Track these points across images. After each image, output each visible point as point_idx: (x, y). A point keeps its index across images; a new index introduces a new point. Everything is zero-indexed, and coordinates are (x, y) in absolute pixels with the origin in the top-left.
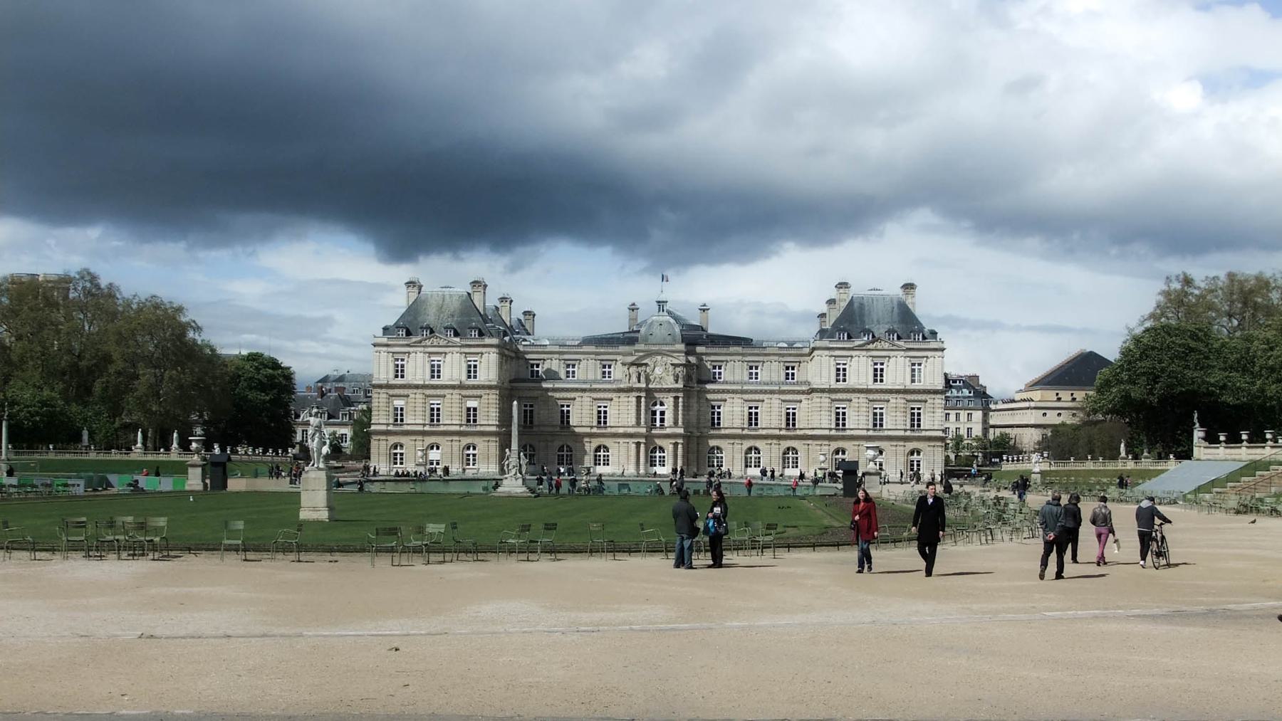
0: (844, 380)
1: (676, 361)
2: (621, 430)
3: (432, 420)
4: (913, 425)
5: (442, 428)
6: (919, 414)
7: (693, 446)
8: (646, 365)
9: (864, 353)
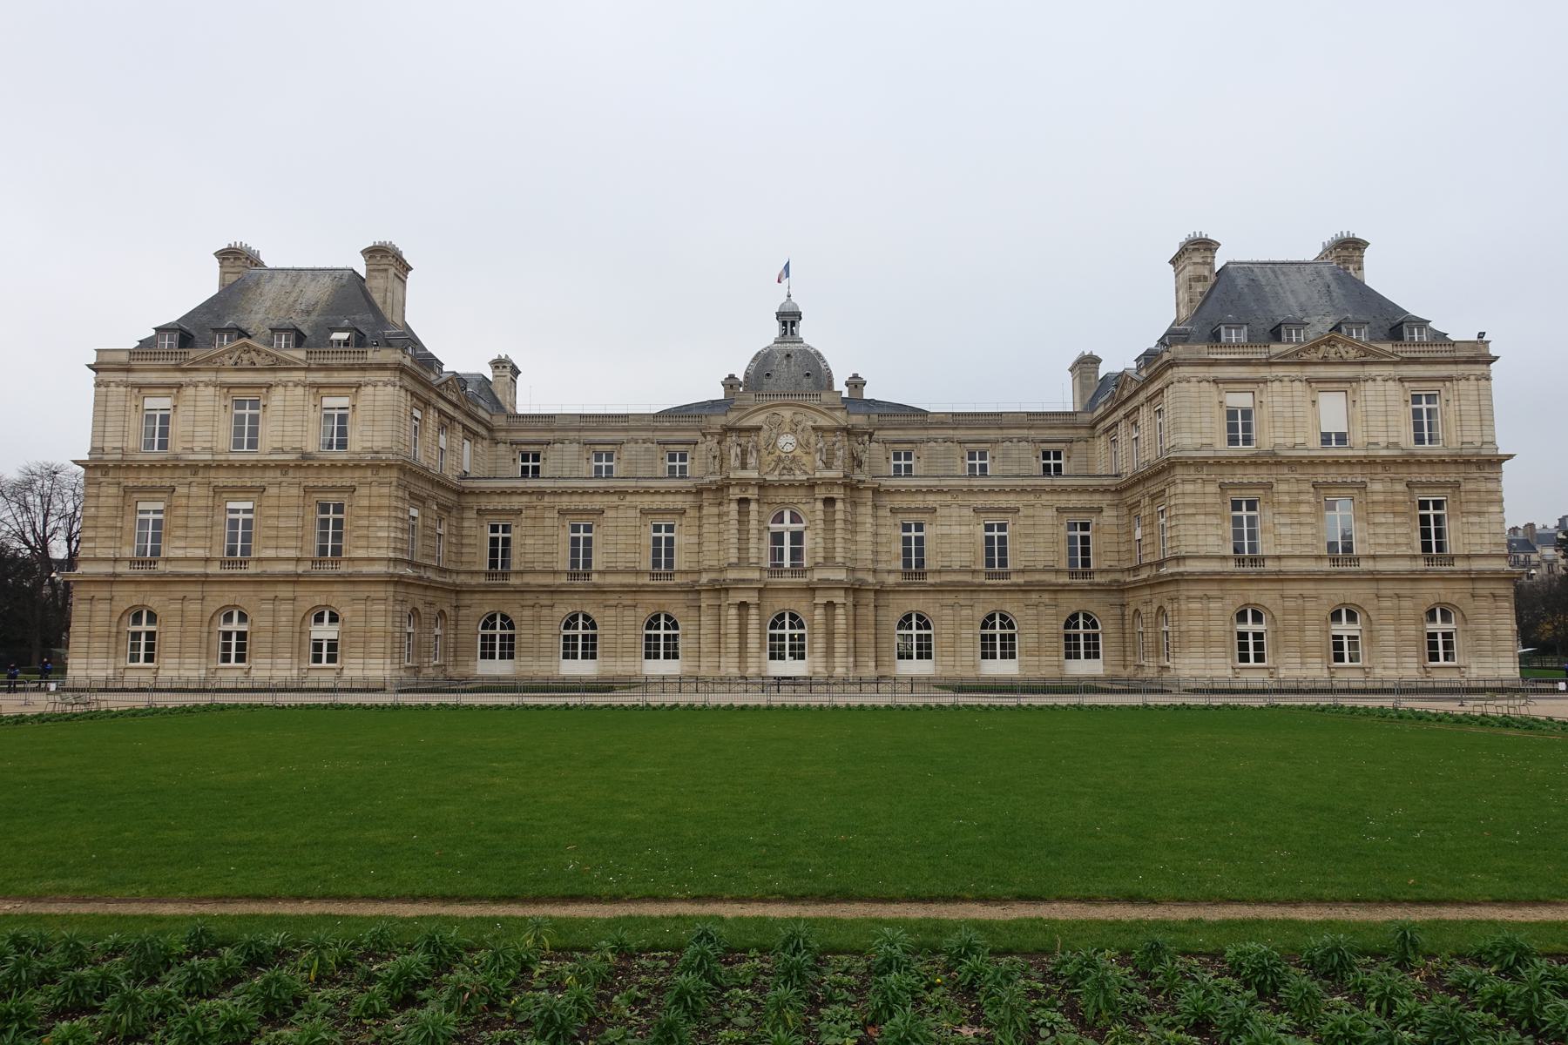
0: (1247, 441)
1: (823, 422)
2: (705, 578)
3: (232, 551)
4: (1426, 547)
5: (252, 568)
6: (1438, 519)
7: (868, 613)
8: (759, 429)
9: (1295, 371)
